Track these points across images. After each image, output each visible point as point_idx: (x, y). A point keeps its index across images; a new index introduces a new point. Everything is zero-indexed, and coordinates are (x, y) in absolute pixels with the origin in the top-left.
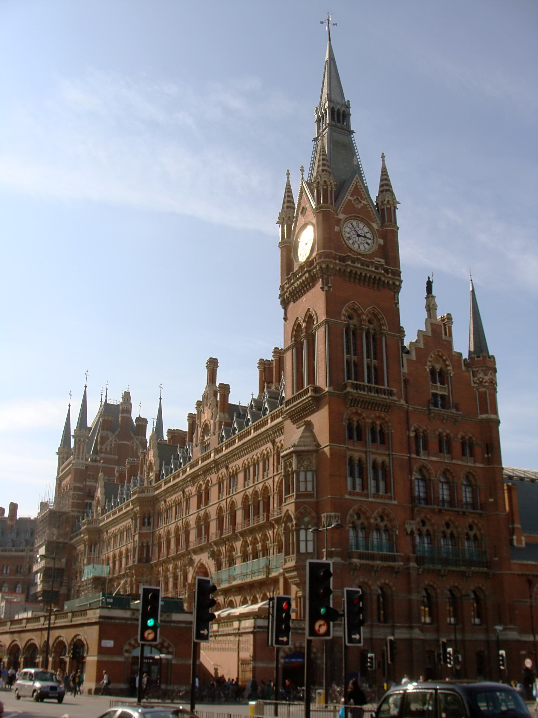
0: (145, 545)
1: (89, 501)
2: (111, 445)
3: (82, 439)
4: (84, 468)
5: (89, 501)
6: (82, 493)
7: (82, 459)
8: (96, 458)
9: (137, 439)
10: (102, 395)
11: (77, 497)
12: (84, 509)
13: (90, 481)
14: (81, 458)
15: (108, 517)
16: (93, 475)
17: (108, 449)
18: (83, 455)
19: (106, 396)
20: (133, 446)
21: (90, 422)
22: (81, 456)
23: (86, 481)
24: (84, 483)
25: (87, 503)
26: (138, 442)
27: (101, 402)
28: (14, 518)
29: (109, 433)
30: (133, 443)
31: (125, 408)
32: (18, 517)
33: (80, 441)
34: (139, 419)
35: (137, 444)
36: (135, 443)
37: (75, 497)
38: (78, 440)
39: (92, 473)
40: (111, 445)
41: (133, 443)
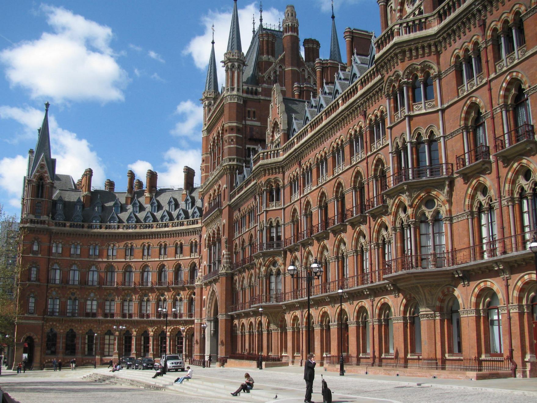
0: (425, 138)
1: (252, 147)
2: (275, 72)
3: (236, 64)
4: (242, 103)
5: (252, 147)
6: (241, 136)
7: (238, 90)
8: (256, 89)
9: (308, 66)
10: (254, 23)
11: (235, 140)
12: (245, 157)
13: (252, 120)
14: (236, 89)
15: (299, 137)
16: (254, 112)
17: (272, 78)
18: (238, 85)
19: (261, 20)
20: (304, 75)
21: (245, 50)
22: (236, 86)
23: (245, 120)
24: (244, 123)
25: (249, 148)
26: (310, 69)
27: (254, 31)
28: (154, 189)
29: (272, 59)
30: (303, 70)
31: (290, 25)
32: (158, 189)
33: (233, 67)
34: (306, 42)
35: (308, 72)
36: (306, 72)
37: (232, 140)
38: (231, 65)
39: (253, 110)
40: (275, 72)
41: (303, 70)
